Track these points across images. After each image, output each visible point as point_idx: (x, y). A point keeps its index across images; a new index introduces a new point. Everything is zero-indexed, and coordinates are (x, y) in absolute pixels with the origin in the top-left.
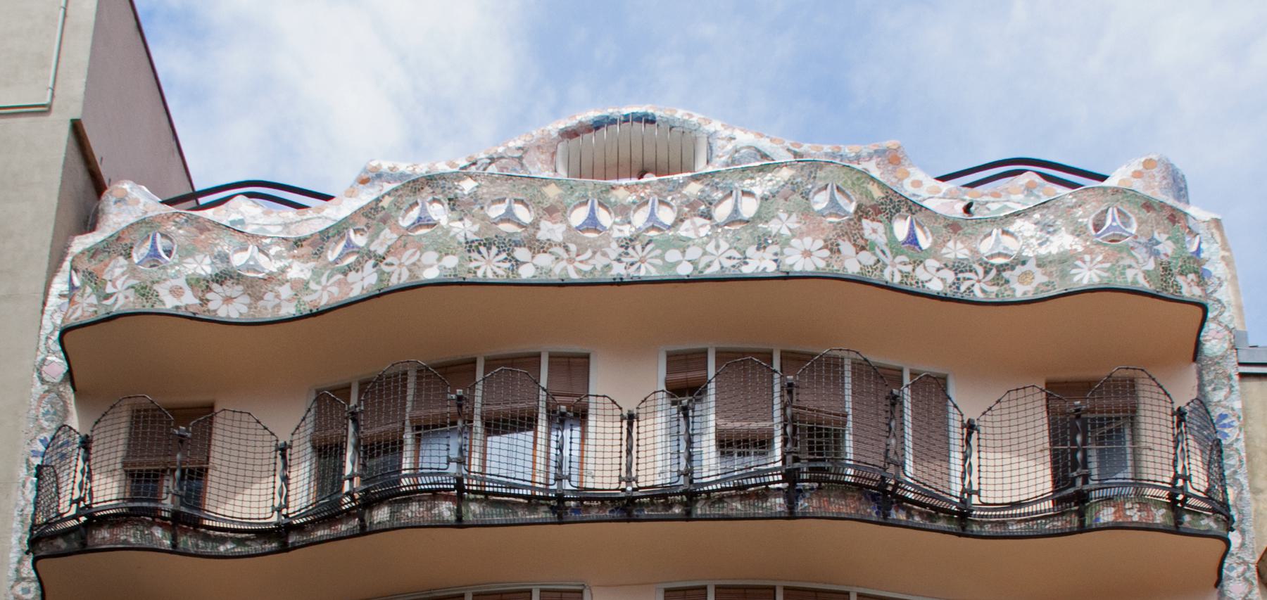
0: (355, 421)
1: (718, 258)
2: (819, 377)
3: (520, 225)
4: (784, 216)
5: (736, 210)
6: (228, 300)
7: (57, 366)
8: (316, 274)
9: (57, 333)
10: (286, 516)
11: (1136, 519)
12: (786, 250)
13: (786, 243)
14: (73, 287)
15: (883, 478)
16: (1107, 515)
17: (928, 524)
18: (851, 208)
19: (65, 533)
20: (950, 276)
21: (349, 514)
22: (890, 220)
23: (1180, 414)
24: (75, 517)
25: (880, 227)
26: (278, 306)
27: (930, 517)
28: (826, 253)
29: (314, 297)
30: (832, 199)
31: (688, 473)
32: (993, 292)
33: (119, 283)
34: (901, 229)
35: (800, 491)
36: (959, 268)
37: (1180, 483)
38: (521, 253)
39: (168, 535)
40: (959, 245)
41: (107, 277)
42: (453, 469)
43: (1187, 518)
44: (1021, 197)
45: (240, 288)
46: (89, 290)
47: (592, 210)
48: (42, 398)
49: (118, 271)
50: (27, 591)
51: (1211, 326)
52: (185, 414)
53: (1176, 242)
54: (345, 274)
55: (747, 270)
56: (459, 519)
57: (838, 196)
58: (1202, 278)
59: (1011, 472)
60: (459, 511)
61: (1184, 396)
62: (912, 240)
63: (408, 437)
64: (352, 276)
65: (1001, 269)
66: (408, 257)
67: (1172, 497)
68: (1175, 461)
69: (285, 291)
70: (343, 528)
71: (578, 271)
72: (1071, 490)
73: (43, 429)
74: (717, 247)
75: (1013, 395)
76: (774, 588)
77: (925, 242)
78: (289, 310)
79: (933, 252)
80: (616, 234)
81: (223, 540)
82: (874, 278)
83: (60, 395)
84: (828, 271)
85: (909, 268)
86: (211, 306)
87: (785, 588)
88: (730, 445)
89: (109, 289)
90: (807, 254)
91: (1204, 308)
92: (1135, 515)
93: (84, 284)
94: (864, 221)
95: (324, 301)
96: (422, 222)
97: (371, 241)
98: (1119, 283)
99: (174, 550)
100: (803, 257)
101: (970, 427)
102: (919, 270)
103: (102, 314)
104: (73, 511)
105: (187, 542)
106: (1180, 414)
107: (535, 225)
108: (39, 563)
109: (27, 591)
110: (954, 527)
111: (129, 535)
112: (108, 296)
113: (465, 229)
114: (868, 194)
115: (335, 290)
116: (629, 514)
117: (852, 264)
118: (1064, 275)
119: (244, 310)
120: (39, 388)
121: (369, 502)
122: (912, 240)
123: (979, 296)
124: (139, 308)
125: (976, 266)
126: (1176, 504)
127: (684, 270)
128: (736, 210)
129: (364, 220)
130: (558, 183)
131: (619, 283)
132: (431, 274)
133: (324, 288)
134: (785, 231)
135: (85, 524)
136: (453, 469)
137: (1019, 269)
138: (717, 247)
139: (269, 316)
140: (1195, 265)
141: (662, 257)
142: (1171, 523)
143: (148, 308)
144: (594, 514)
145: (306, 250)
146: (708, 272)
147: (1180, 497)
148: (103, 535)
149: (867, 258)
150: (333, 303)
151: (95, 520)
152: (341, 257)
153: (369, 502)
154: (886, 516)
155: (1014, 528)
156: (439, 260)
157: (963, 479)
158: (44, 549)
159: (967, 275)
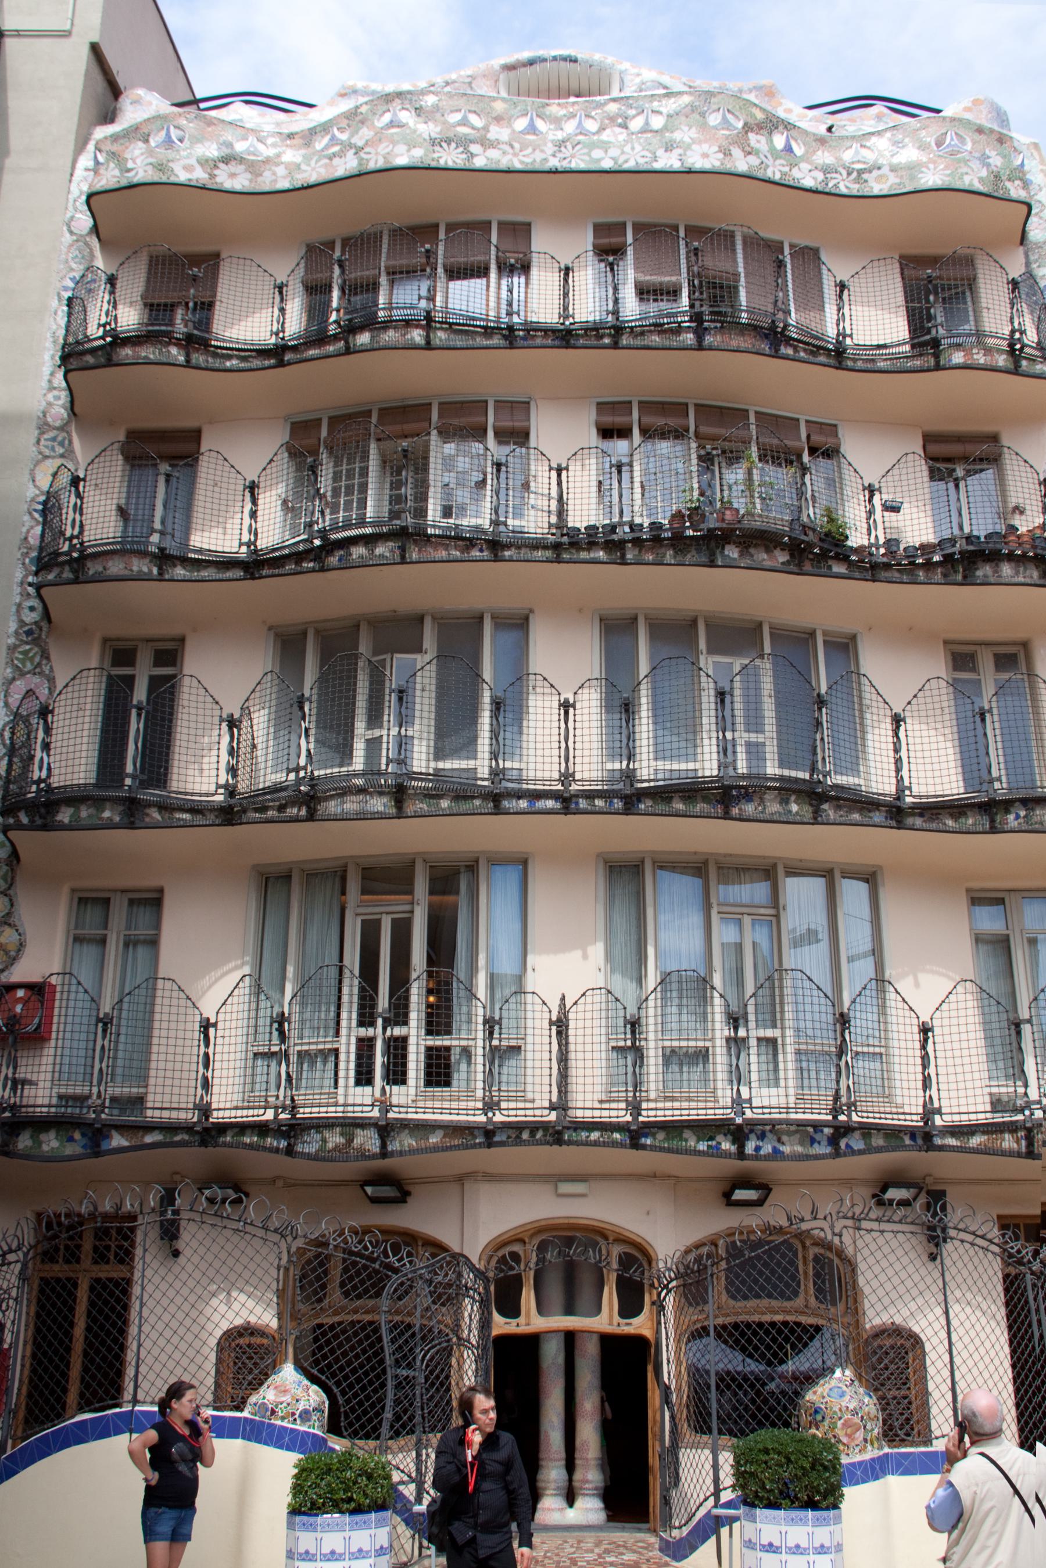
0: (341, 266)
1: (634, 158)
2: (719, 245)
3: (473, 128)
4: (686, 129)
5: (647, 123)
6: (233, 175)
7: (84, 221)
8: (307, 159)
9: (84, 198)
10: (283, 339)
11: (982, 361)
12: (689, 153)
13: (688, 147)
14: (97, 162)
15: (773, 322)
16: (958, 358)
17: (811, 358)
18: (740, 125)
19: (93, 351)
20: (820, 176)
21: (335, 338)
22: (770, 134)
23: (1014, 284)
24: (103, 338)
25: (763, 139)
26: (275, 181)
27: (812, 353)
28: (721, 156)
29: (305, 175)
30: (724, 117)
31: (616, 313)
32: (855, 189)
33: (138, 161)
35: (706, 329)
36: (826, 170)
37: (1017, 335)
39: (182, 352)
40: (826, 154)
41: (127, 156)
42: (423, 304)
43: (1024, 363)
44: (872, 122)
45: (243, 167)
46: (112, 165)
47: (532, 119)
48: (71, 245)
49: (137, 152)
50: (58, 398)
51: (1033, 220)
52: (196, 259)
53: (1004, 157)
54: (331, 159)
55: (657, 166)
56: (428, 342)
57: (729, 117)
58: (1026, 185)
59: (875, 319)
60: (428, 336)
61: (1016, 271)
62: (788, 149)
63: (383, 280)
64: (336, 161)
65: (860, 172)
66: (383, 148)
67: (1011, 345)
68: (1012, 318)
69: (281, 171)
70: (331, 349)
72: (928, 337)
73: (72, 270)
74: (633, 149)
75: (876, 264)
76: (687, 405)
77: (798, 150)
78: (284, 184)
79: (805, 158)
80: (551, 137)
81: (230, 357)
82: (760, 174)
83: (86, 244)
84: (722, 169)
85: (787, 169)
86: (218, 180)
87: (696, 405)
88: (648, 292)
89: (130, 165)
90: (705, 156)
91: (1029, 207)
92: (980, 358)
93: (107, 161)
94: (751, 135)
95: (313, 179)
96: (392, 124)
97: (352, 135)
98: (958, 185)
99: (188, 364)
100: (703, 157)
101: (842, 286)
103: (124, 183)
104: (101, 333)
105: (199, 358)
106: (1014, 284)
107: (486, 129)
108: (70, 375)
109: (58, 398)
110: (832, 362)
111: (148, 352)
112: (129, 170)
113: (428, 129)
115: (323, 171)
116: (568, 342)
117: (742, 164)
118: (912, 178)
119: (246, 183)
120: (68, 238)
121: (350, 329)
122: (788, 149)
123: (844, 190)
124: (156, 179)
125: (840, 169)
126: (1015, 351)
127: (607, 164)
128: (647, 123)
129: (346, 121)
130: (503, 100)
133: (313, 169)
135: (111, 344)
136: (423, 304)
138: (633, 149)
139: (267, 188)
140: (1019, 174)
142: (1011, 366)
143: (164, 179)
144: (539, 341)
145: (297, 141)
146: (626, 166)
147: (1018, 346)
148: (127, 352)
149: (753, 160)
150: (321, 180)
151: (118, 341)
152: (327, 147)
153: (350, 329)
154: (777, 351)
155: (881, 365)
156: (409, 151)
157: (838, 325)
158: (74, 363)
159: (834, 175)
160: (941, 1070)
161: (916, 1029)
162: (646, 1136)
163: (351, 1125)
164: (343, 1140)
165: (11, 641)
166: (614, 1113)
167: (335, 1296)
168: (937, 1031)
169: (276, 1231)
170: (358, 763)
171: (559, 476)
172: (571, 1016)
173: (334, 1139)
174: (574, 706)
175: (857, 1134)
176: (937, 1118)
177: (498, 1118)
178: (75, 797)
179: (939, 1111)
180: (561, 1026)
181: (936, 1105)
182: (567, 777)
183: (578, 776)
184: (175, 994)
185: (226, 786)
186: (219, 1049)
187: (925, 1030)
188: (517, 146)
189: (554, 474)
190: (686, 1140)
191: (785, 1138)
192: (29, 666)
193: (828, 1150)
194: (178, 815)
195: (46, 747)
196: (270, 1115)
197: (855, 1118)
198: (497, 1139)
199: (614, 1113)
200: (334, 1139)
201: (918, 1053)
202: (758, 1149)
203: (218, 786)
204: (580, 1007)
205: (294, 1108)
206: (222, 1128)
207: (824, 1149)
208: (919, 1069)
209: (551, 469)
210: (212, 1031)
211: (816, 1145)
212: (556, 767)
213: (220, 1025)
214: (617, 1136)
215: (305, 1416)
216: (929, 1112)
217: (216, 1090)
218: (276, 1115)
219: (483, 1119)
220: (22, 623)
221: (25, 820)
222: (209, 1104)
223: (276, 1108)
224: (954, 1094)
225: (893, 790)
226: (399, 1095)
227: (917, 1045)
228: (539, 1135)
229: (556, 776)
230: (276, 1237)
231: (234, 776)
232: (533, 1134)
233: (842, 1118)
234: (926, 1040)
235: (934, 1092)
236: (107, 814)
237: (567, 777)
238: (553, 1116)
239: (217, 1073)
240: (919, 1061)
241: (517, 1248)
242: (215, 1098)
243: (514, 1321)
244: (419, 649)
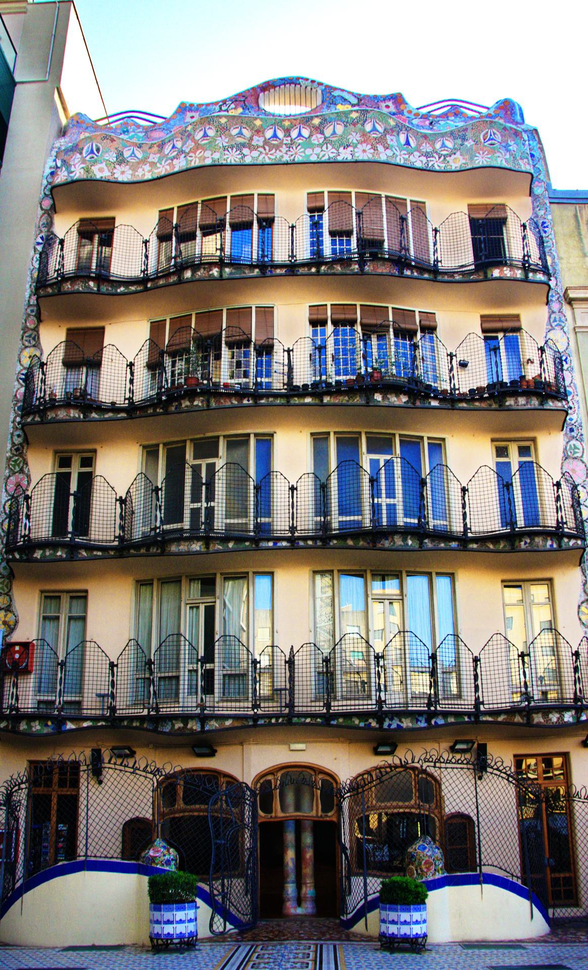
34: (402, 138)
38: (246, 151)
71: (269, 159)
102: (411, 157)
114: (389, 124)
131: (287, 164)
132: (208, 162)
134: (355, 141)
137: (453, 157)
141: (304, 152)
160: (484, 682)
161: (471, 660)
163: (185, 718)
164: (181, 725)
165: (9, 454)
166: (317, 709)
167: (180, 804)
168: (482, 661)
169: (151, 773)
170: (186, 524)
172: (296, 658)
173: (179, 725)
174: (296, 489)
175: (440, 717)
176: (482, 706)
177: (260, 712)
178: (43, 545)
179: (482, 703)
180: (291, 663)
181: (481, 700)
182: (293, 529)
183: (299, 528)
184: (96, 650)
185: (119, 537)
186: (119, 678)
187: (476, 660)
188: (267, 148)
189: (286, 353)
191: (403, 720)
192: (17, 469)
193: (426, 725)
195: (28, 517)
196: (145, 712)
197: (438, 708)
198: (259, 722)
199: (317, 709)
200: (179, 725)
201: (472, 673)
202: (390, 725)
203: (115, 537)
204: (300, 654)
205: (157, 709)
206: (122, 718)
207: (423, 724)
208: (473, 681)
209: (284, 351)
210: (115, 668)
212: (287, 523)
213: (119, 666)
214: (319, 720)
215: (168, 862)
216: (478, 703)
217: (118, 699)
218: (149, 712)
219: (252, 713)
220: (13, 444)
221: (18, 556)
222: (115, 707)
223: (149, 709)
224: (490, 694)
225: (462, 530)
226: (208, 700)
227: (472, 669)
228: (280, 720)
229: (287, 528)
230: (151, 776)
231: (124, 531)
232: (277, 721)
233: (432, 708)
234: (476, 666)
235: (480, 693)
236: (59, 553)
237: (293, 529)
238: (287, 711)
239: (118, 691)
240: (472, 677)
241: (270, 777)
242: (118, 704)
243: (269, 816)
244: (216, 455)
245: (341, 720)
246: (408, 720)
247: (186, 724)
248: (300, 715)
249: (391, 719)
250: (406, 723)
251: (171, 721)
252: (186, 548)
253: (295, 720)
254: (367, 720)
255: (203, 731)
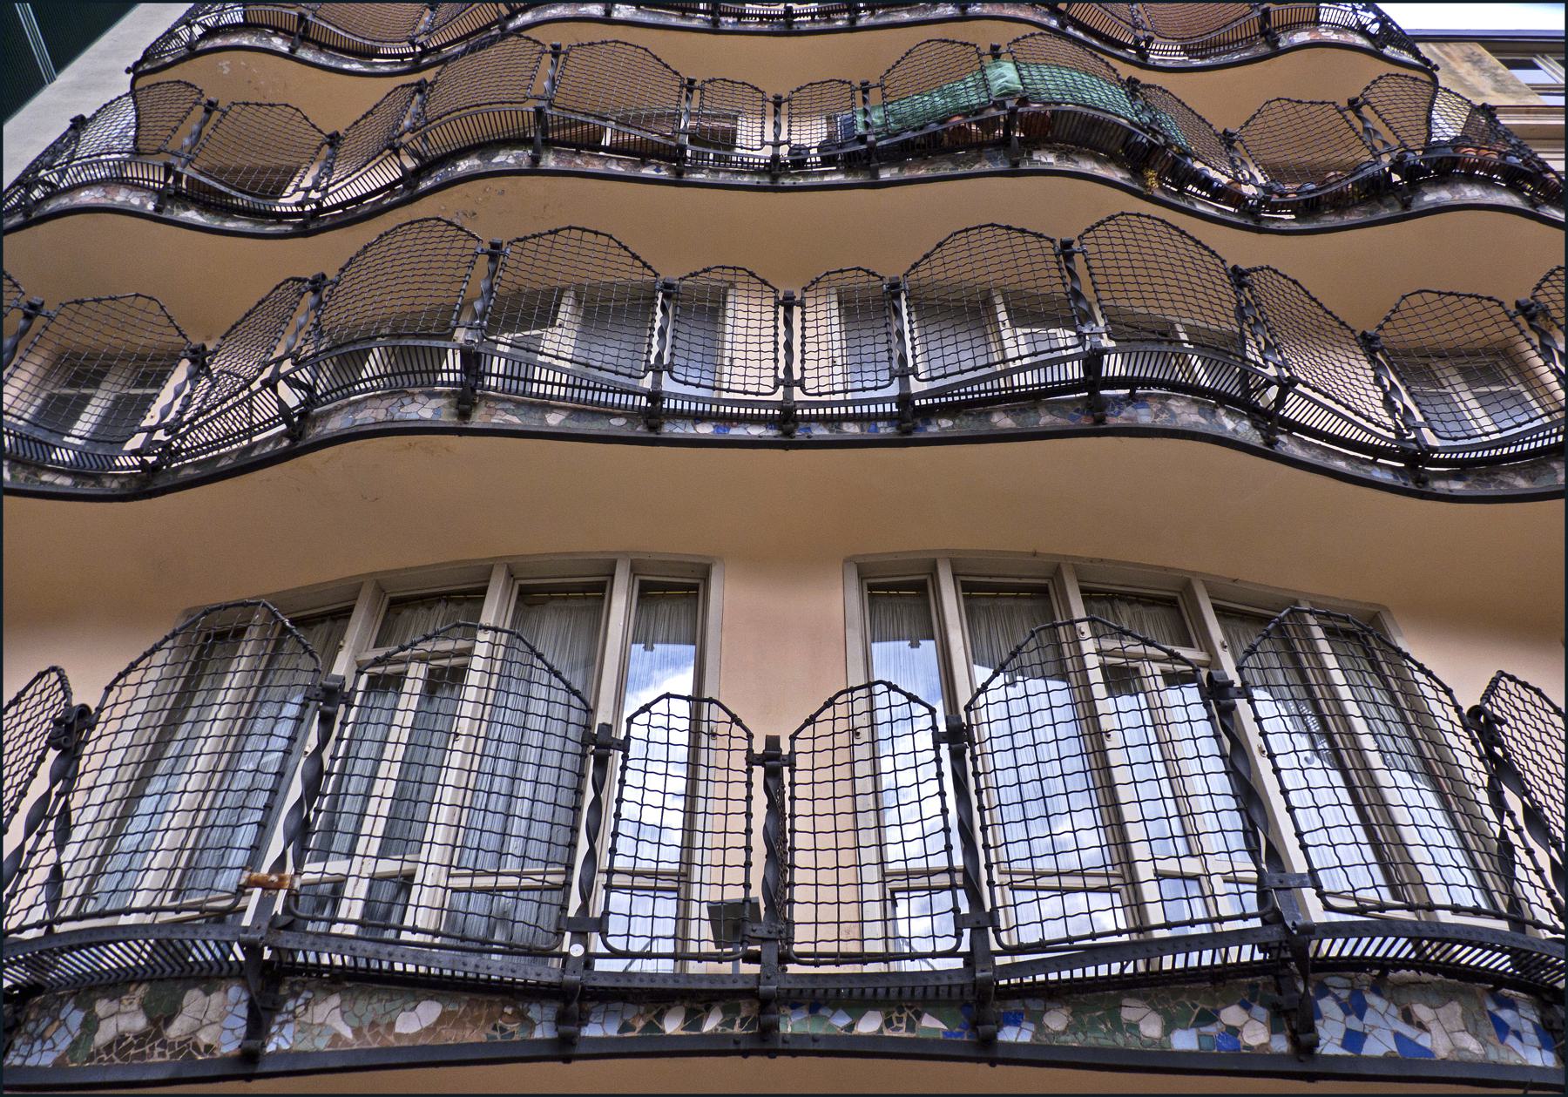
162: (1016, 1021)
164: (140, 1023)
171: (788, 370)
190: (1134, 1026)
191: (1422, 1012)
194: (46, 478)
198: (592, 1031)
202: (1353, 1039)
211: (1511, 1040)
214: (931, 1024)
228: (711, 1025)
245: (1057, 1021)
246: (1454, 1011)
247: (161, 1017)
248: (816, 998)
249: (1355, 1007)
250: (1447, 1035)
251: (86, 1004)
252: (382, 415)
253: (792, 1024)
254: (1209, 1017)
255: (249, 1062)
